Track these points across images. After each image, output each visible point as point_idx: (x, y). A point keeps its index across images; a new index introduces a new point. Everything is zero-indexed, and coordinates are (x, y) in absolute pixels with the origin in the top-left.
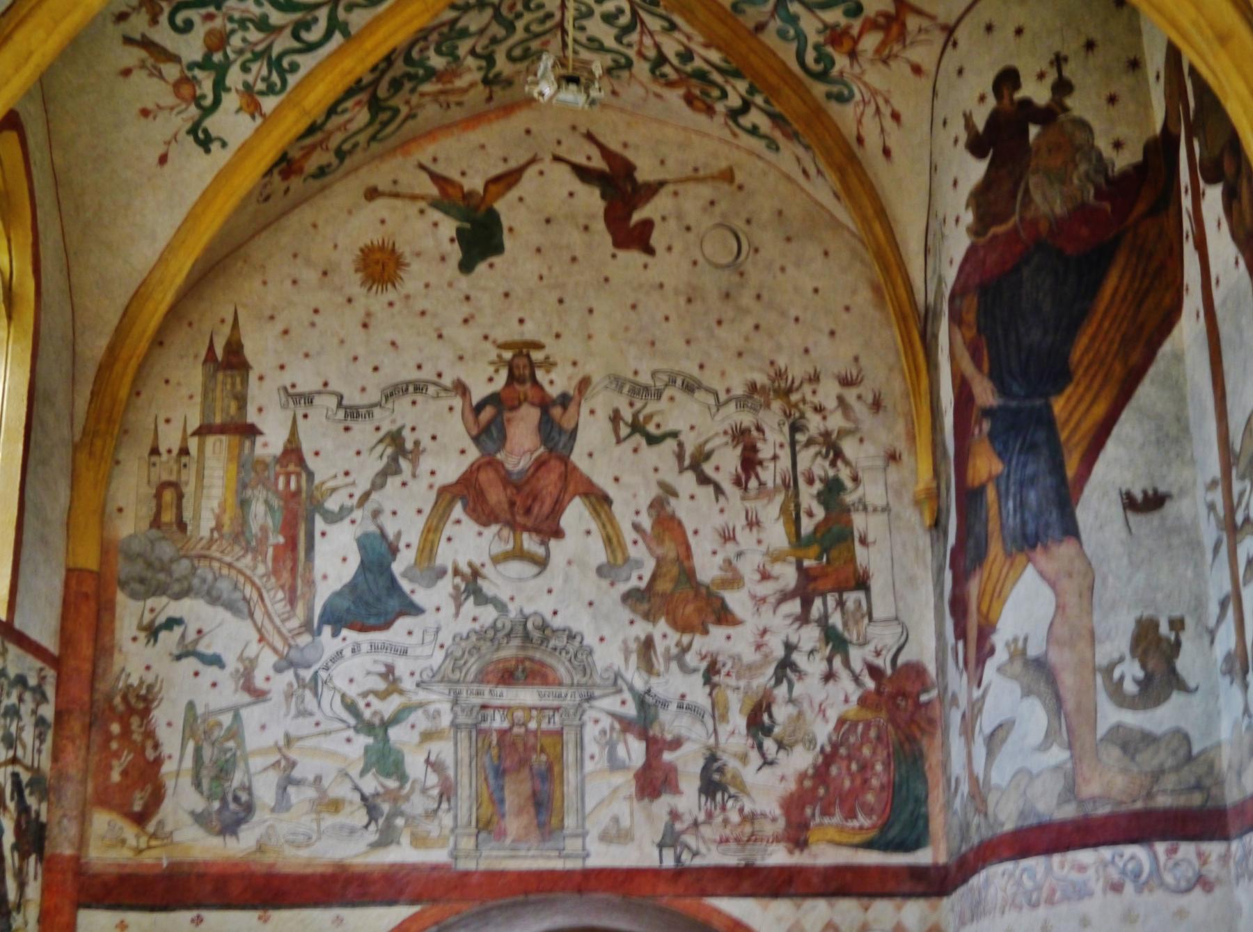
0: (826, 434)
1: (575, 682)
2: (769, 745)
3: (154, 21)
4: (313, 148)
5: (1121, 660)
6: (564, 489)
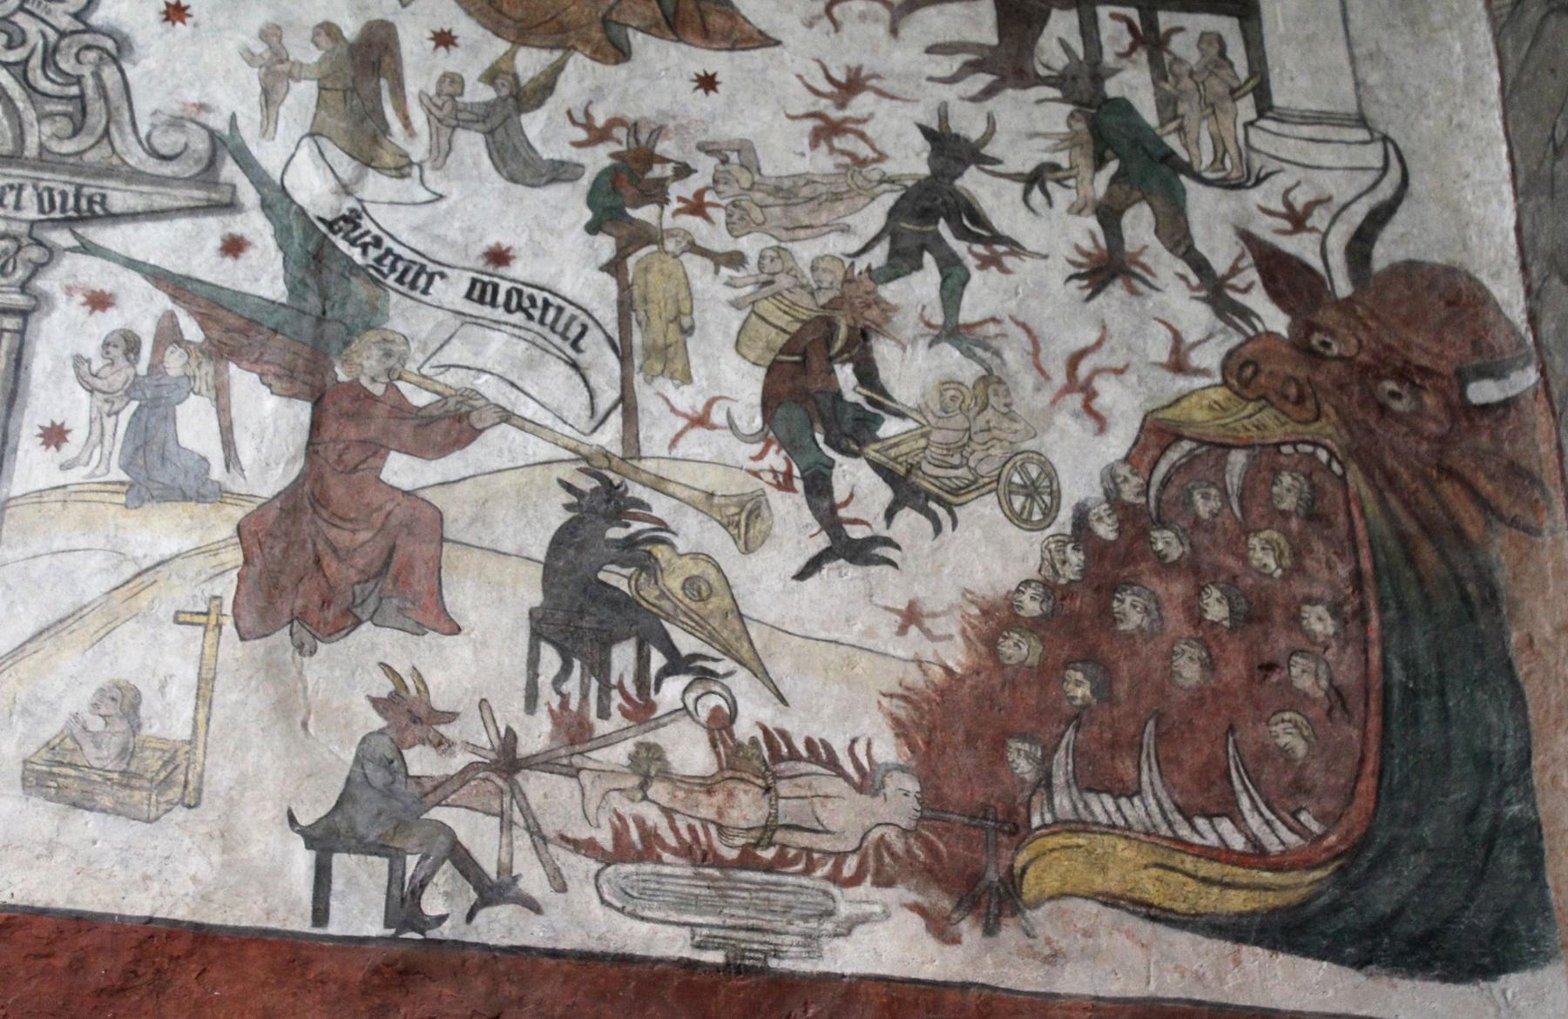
1: (31, 150)
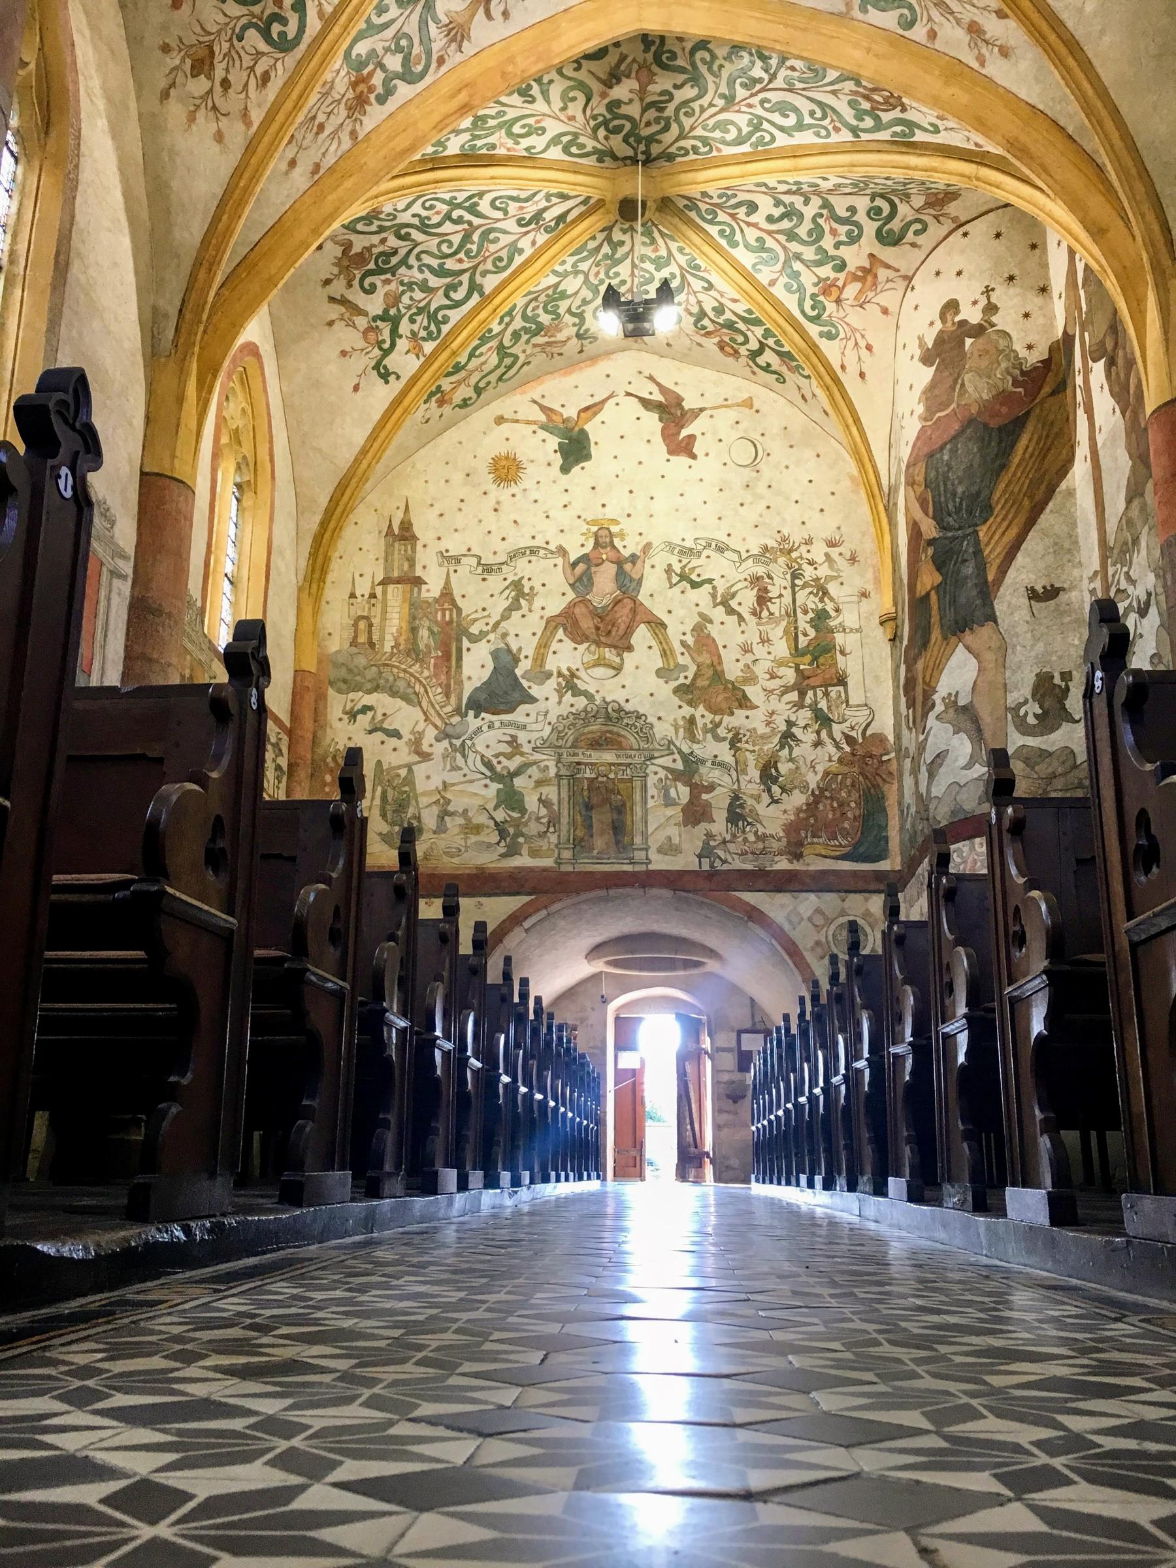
0: (818, 579)
2: (776, 789)
3: (349, 285)
4: (459, 383)
5: (1026, 702)
6: (633, 620)
